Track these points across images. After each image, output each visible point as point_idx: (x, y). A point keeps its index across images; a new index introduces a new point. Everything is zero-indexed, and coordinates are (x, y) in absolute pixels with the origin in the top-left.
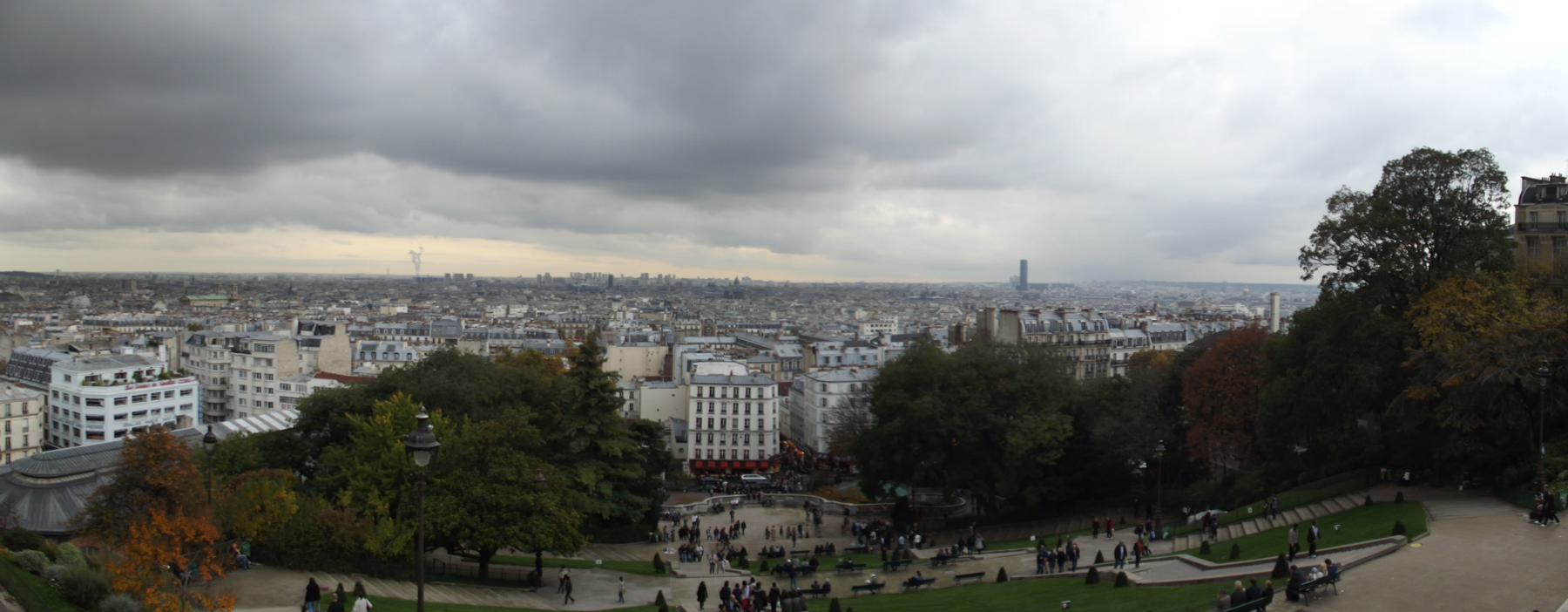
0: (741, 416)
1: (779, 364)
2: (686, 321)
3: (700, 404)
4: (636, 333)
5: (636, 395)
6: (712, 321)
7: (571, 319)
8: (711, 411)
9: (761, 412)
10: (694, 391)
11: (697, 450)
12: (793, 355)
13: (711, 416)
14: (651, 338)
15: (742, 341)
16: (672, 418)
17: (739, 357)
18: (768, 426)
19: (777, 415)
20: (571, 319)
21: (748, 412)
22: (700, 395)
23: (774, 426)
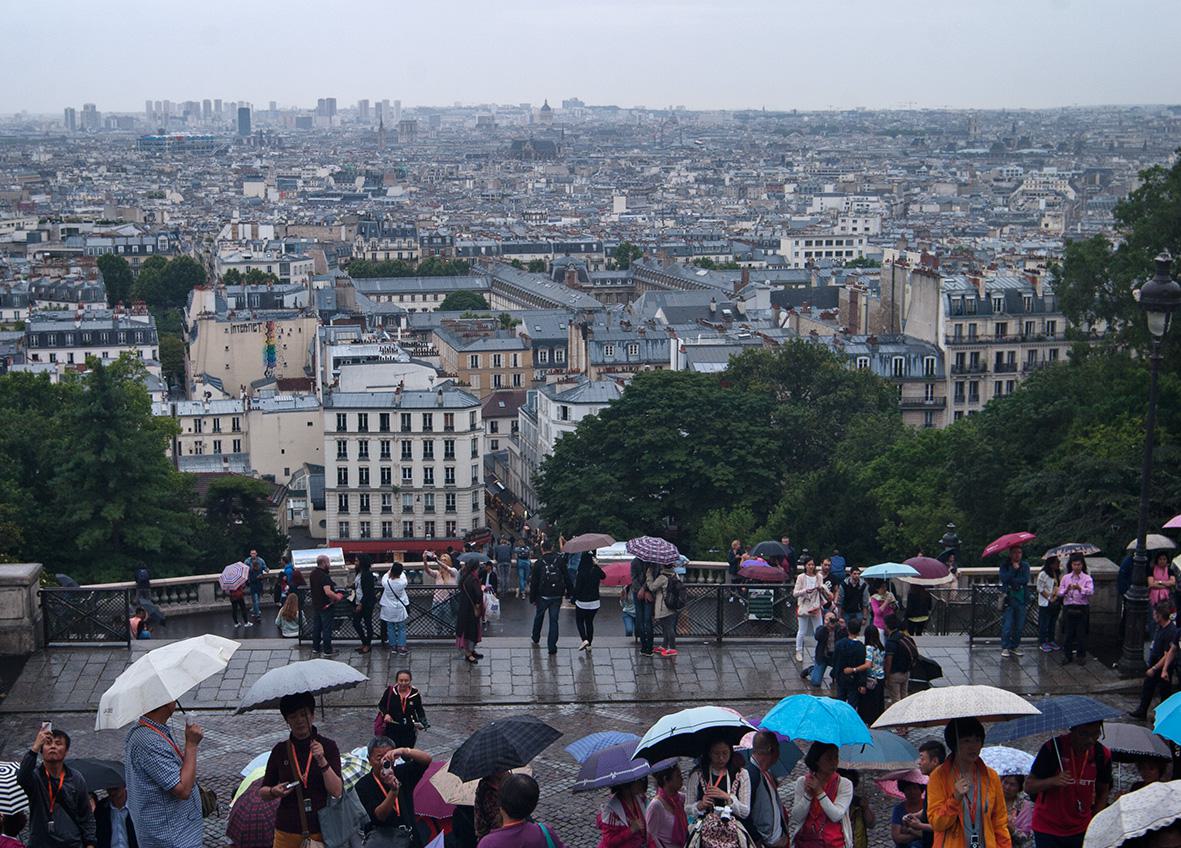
0: (418, 464)
1: (531, 352)
2: (386, 242)
3: (342, 445)
4: (263, 289)
5: (240, 425)
6: (443, 239)
7: (135, 248)
8: (364, 455)
9: (449, 455)
10: (330, 421)
11: (341, 523)
12: (559, 335)
13: (363, 464)
14: (288, 301)
15: (501, 285)
16: (308, 465)
17: (425, 354)
18: (463, 479)
19: (480, 461)
20: (135, 248)
21: (428, 454)
22: (342, 428)
23: (475, 479)
